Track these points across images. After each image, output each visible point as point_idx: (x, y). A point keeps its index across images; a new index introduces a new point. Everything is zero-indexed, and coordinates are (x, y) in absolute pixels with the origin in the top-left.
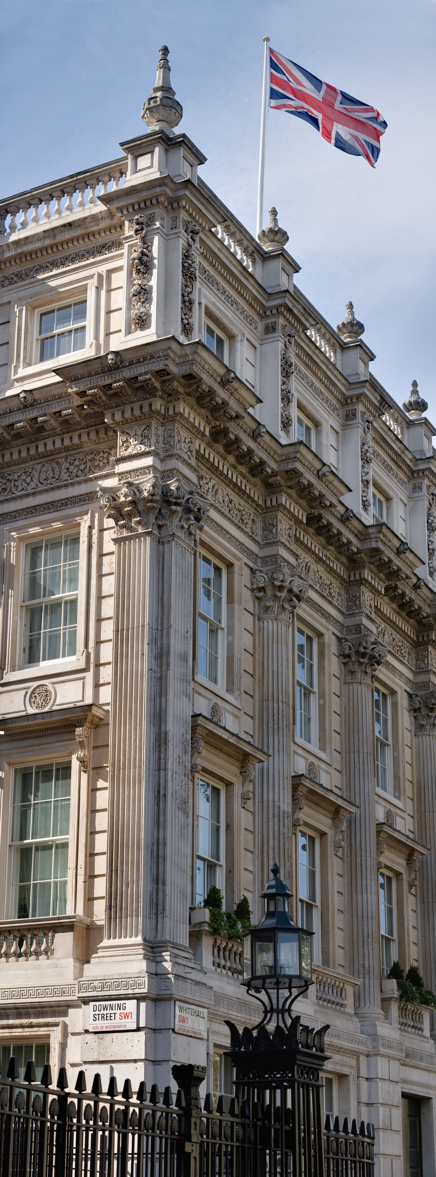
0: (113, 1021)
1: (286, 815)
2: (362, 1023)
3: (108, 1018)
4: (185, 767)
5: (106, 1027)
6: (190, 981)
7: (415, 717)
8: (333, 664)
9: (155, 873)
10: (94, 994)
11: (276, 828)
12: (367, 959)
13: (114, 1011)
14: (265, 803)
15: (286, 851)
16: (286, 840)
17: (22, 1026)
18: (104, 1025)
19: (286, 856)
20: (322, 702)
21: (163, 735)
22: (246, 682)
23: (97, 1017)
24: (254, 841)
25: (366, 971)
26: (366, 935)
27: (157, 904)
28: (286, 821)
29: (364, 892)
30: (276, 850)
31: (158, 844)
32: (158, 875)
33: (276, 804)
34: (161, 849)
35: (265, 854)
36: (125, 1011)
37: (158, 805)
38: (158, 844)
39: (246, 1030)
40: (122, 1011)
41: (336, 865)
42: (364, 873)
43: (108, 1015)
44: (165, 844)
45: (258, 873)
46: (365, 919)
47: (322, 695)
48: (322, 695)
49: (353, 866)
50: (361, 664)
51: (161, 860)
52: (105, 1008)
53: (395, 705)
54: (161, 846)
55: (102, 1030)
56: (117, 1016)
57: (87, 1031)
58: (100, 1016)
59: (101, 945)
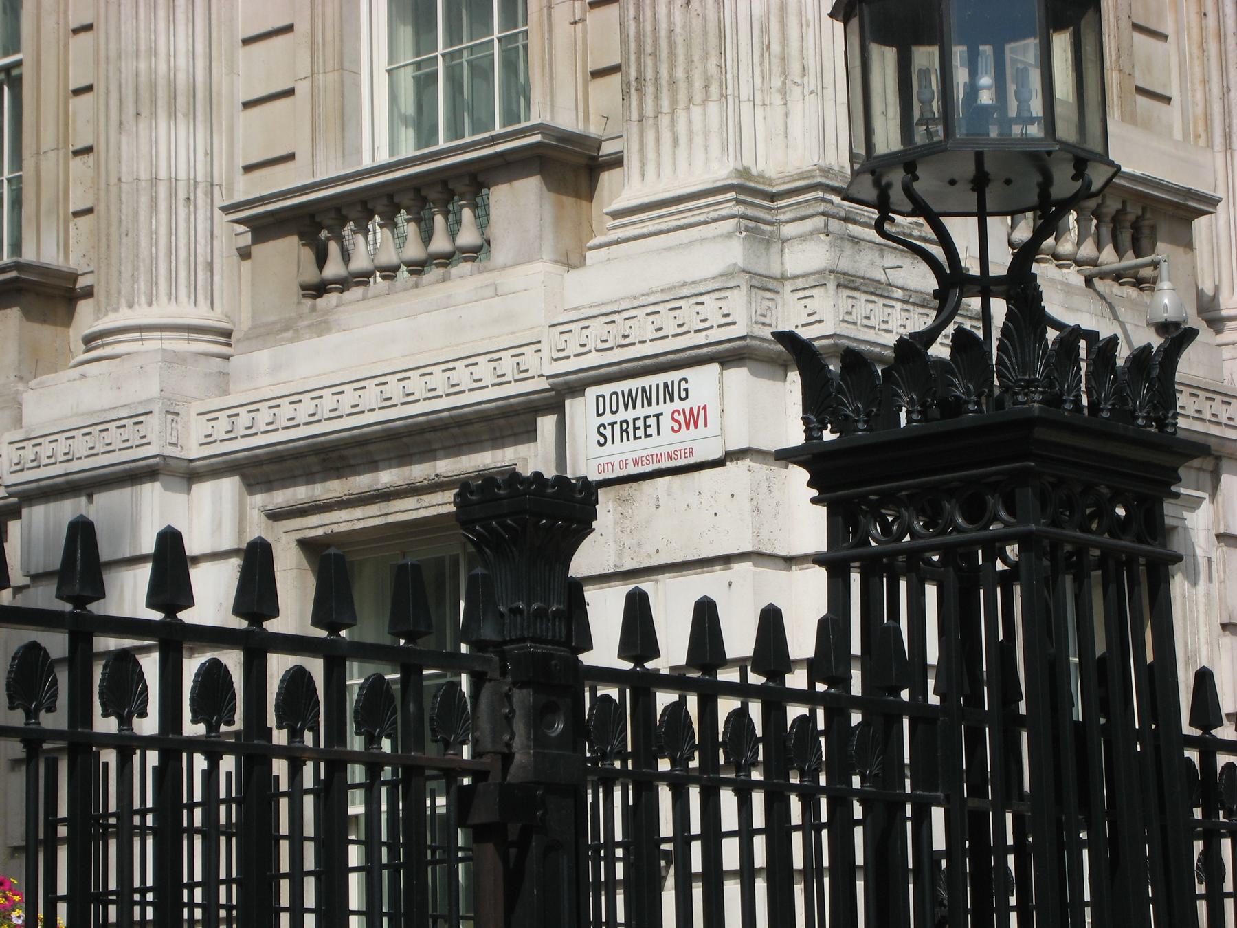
0: (655, 440)
3: (640, 433)
5: (636, 463)
6: (899, 294)
10: (593, 359)
17: (413, 490)
18: (631, 457)
23: (608, 432)
27: (784, 59)
36: (686, 405)
40: (678, 404)
43: (640, 423)
52: (630, 400)
55: (624, 473)
56: (666, 422)
58: (617, 427)
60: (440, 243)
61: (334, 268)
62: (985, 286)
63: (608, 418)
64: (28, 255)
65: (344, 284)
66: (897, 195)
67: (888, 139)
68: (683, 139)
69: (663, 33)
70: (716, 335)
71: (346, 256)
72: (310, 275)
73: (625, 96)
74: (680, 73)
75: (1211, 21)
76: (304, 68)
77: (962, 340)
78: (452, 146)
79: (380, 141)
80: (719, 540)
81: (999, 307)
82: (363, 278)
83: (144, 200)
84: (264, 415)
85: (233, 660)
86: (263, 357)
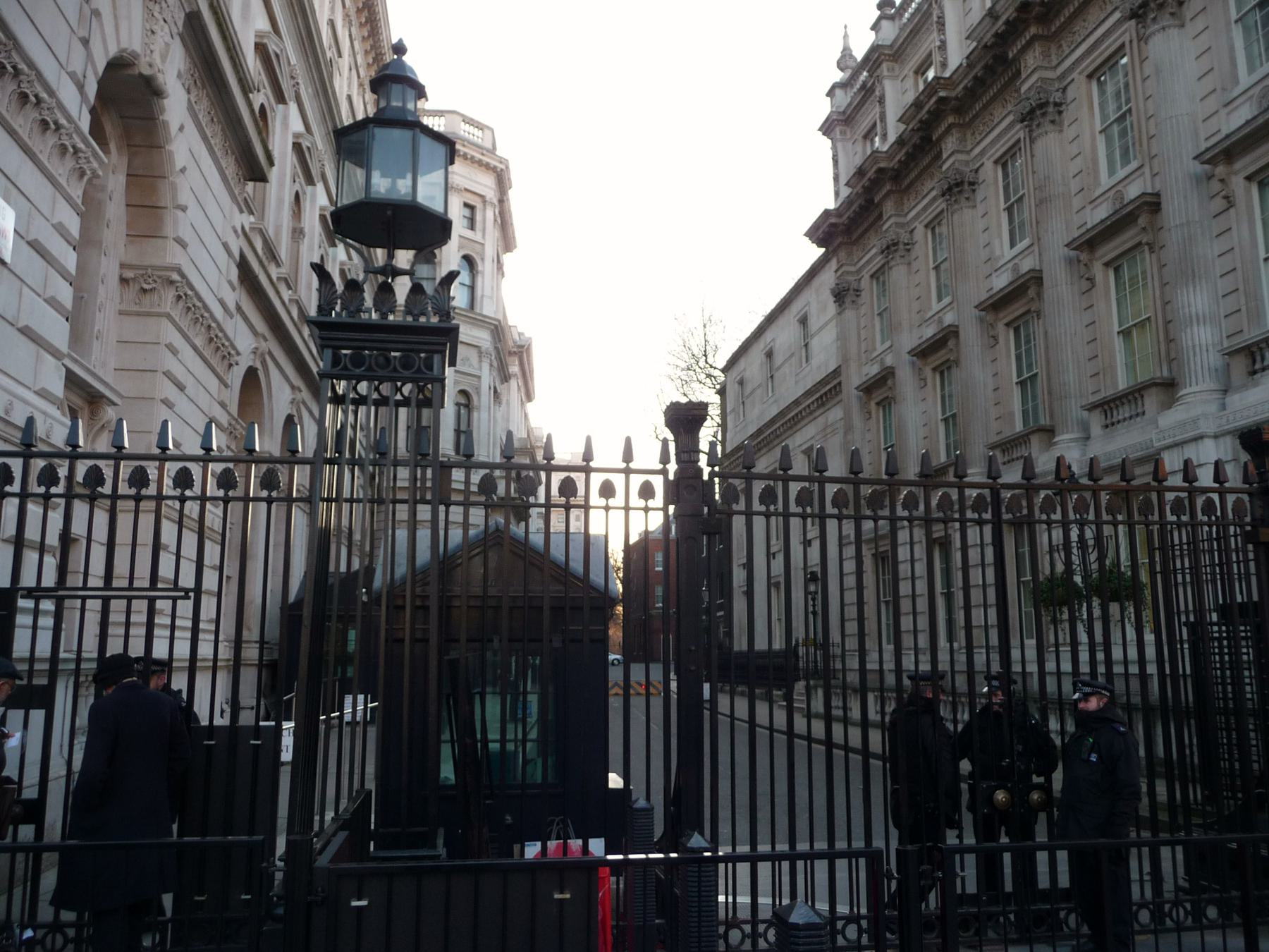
61: (1258, 366)
71: (1263, 359)
72: (1250, 369)
76: (1243, 301)
83: (1191, 354)
84: (1238, 416)
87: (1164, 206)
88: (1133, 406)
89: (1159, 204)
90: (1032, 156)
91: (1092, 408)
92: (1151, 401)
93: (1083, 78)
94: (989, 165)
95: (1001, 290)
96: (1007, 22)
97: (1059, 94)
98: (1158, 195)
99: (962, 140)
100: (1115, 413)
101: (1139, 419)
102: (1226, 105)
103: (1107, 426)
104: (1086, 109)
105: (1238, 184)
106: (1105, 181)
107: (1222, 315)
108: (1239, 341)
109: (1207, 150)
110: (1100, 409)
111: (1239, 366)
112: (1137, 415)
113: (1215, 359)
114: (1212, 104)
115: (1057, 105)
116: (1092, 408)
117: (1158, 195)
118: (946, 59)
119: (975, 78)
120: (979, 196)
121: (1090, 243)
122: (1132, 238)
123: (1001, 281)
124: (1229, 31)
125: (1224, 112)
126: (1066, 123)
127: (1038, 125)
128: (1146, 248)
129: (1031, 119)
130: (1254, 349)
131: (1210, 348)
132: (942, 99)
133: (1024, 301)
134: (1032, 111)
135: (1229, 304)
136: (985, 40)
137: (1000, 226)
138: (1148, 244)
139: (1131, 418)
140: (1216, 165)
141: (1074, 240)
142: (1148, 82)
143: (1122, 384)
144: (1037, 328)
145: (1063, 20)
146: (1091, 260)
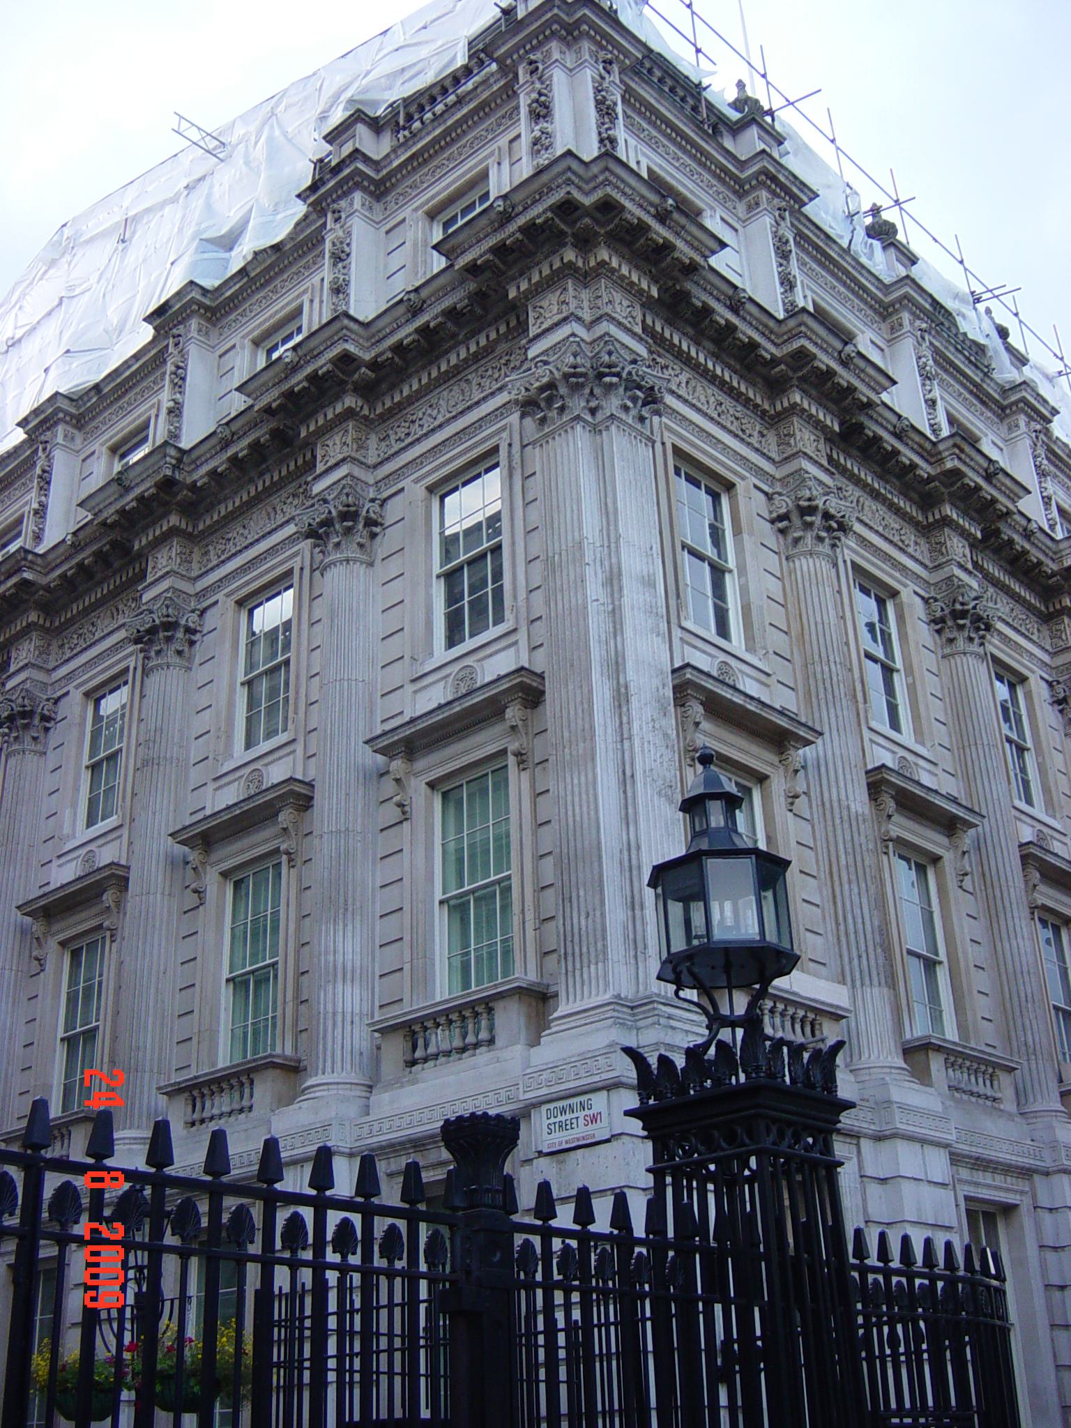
1: (860, 818)
2: (1032, 1127)
4: (666, 735)
7: (1061, 711)
8: (922, 633)
9: (629, 894)
10: (544, 1091)
11: (848, 838)
12: (1029, 1033)
13: (575, 1115)
14: (827, 805)
15: (868, 870)
16: (865, 853)
19: (868, 878)
20: (910, 680)
21: (623, 690)
22: (777, 641)
24: (817, 861)
25: (1031, 1051)
26: (1023, 999)
27: (635, 941)
28: (862, 827)
29: (1012, 936)
30: (852, 869)
31: (629, 850)
32: (633, 897)
33: (844, 803)
34: (634, 856)
35: (836, 878)
36: (591, 1112)
37: (625, 792)
38: (629, 850)
39: (663, 1060)
40: (587, 1112)
41: (963, 904)
42: (1008, 909)
44: (638, 848)
45: (828, 906)
46: (1019, 975)
47: (909, 671)
48: (909, 671)
49: (992, 904)
50: (961, 628)
51: (635, 872)
52: (563, 1111)
53: (1028, 696)
54: (634, 852)
56: (581, 1121)
57: (540, 1154)
59: (556, 1015)
60: (471, 1039)
61: (419, 1053)
62: (732, 1023)
63: (552, 1120)
64: (278, 1051)
65: (426, 1060)
66: (685, 977)
67: (679, 945)
68: (587, 983)
69: (576, 930)
70: (604, 1076)
71: (426, 1046)
72: (409, 1058)
73: (559, 962)
74: (584, 950)
75: (842, 927)
76: (407, 958)
77: (721, 1045)
78: (477, 990)
79: (443, 989)
80: (599, 1161)
81: (740, 1032)
82: (436, 1056)
83: (330, 1023)
84: (386, 1126)
85: (307, 1213)
86: (386, 1097)
87: (315, 802)
88: (237, 1095)
89: (312, 798)
90: (142, 697)
91: (174, 1092)
92: (264, 1089)
93: (230, 603)
94: (76, 696)
95: (62, 887)
96: (140, 499)
97: (194, 617)
98: (310, 785)
99: (44, 651)
100: (208, 1104)
101: (243, 1116)
102: (413, 681)
103: (193, 1124)
104: (228, 645)
105: (417, 789)
106: (240, 754)
107: (378, 973)
108: (395, 1014)
109: (385, 734)
110: (186, 1094)
111: (395, 1049)
112: (241, 1111)
113: (360, 1038)
114: (398, 674)
115: (189, 631)
116: (174, 1092)
117: (310, 785)
118: (42, 530)
119: (80, 565)
120: (54, 738)
121: (206, 837)
122: (266, 841)
123: (64, 874)
124: (428, 586)
125: (410, 688)
126: (197, 661)
127: (158, 653)
128: (284, 858)
129: (151, 642)
130: (417, 1028)
131: (357, 1019)
132: (25, 582)
133: (94, 910)
134: (153, 631)
135: (390, 958)
136: (105, 515)
137: (76, 789)
138: (288, 853)
139: (230, 1113)
140: (392, 758)
141: (185, 828)
142: (317, 628)
143: (224, 1059)
144: (111, 954)
145: (216, 517)
146: (203, 863)
